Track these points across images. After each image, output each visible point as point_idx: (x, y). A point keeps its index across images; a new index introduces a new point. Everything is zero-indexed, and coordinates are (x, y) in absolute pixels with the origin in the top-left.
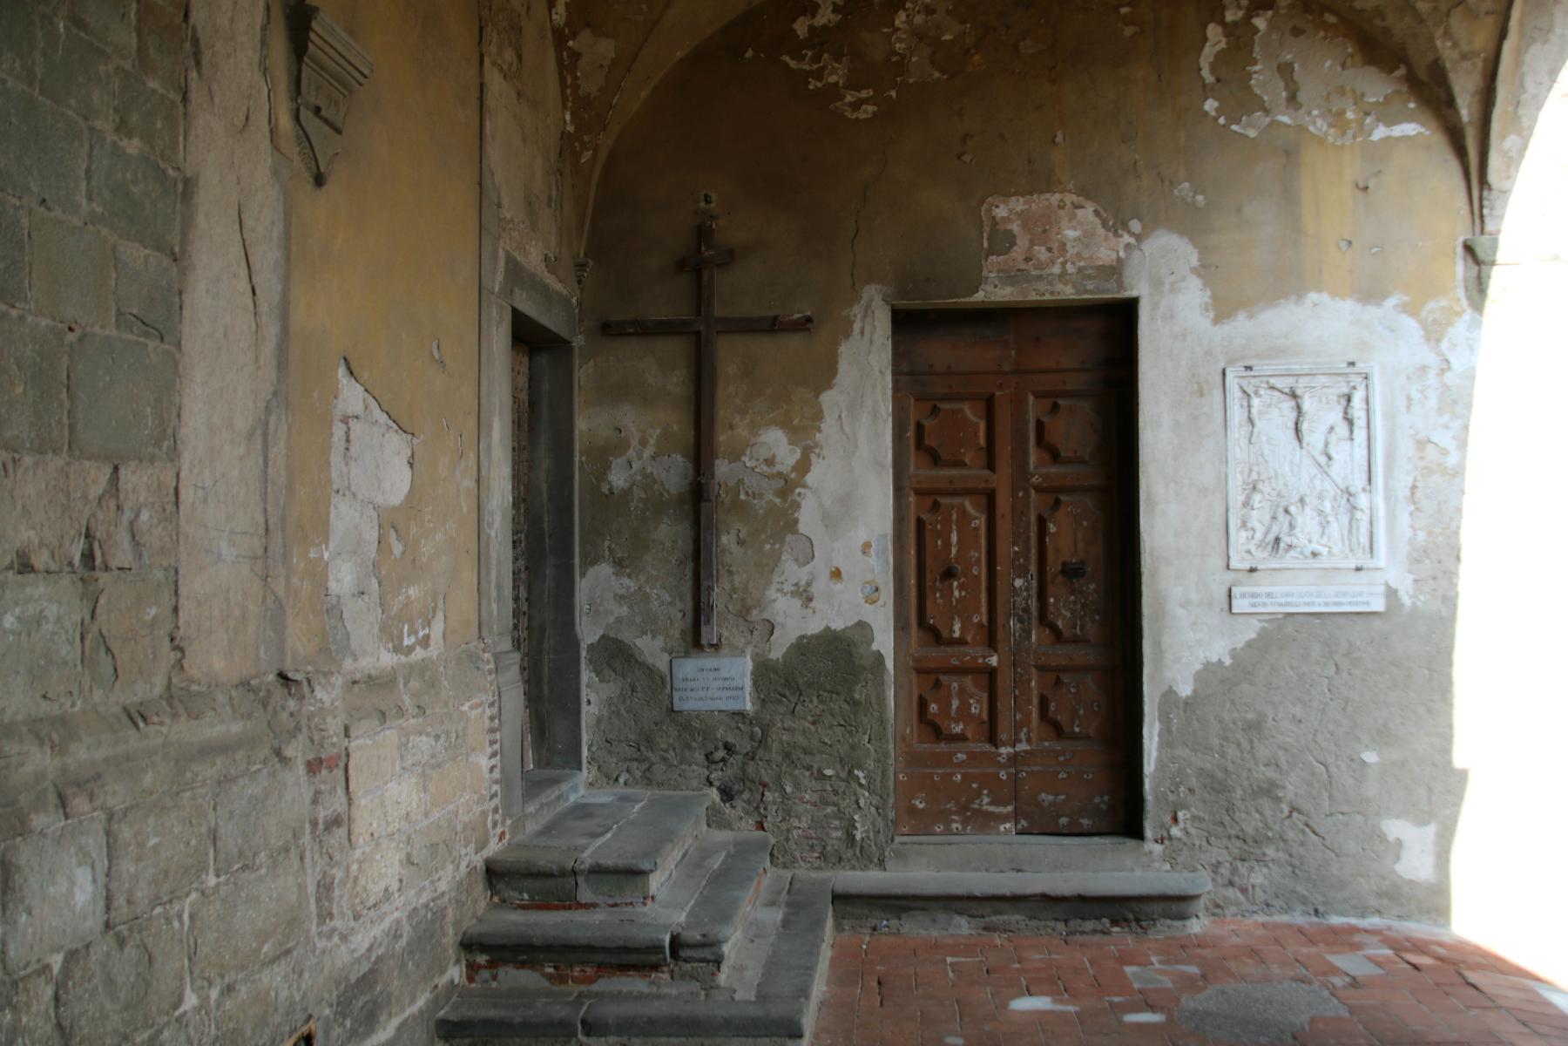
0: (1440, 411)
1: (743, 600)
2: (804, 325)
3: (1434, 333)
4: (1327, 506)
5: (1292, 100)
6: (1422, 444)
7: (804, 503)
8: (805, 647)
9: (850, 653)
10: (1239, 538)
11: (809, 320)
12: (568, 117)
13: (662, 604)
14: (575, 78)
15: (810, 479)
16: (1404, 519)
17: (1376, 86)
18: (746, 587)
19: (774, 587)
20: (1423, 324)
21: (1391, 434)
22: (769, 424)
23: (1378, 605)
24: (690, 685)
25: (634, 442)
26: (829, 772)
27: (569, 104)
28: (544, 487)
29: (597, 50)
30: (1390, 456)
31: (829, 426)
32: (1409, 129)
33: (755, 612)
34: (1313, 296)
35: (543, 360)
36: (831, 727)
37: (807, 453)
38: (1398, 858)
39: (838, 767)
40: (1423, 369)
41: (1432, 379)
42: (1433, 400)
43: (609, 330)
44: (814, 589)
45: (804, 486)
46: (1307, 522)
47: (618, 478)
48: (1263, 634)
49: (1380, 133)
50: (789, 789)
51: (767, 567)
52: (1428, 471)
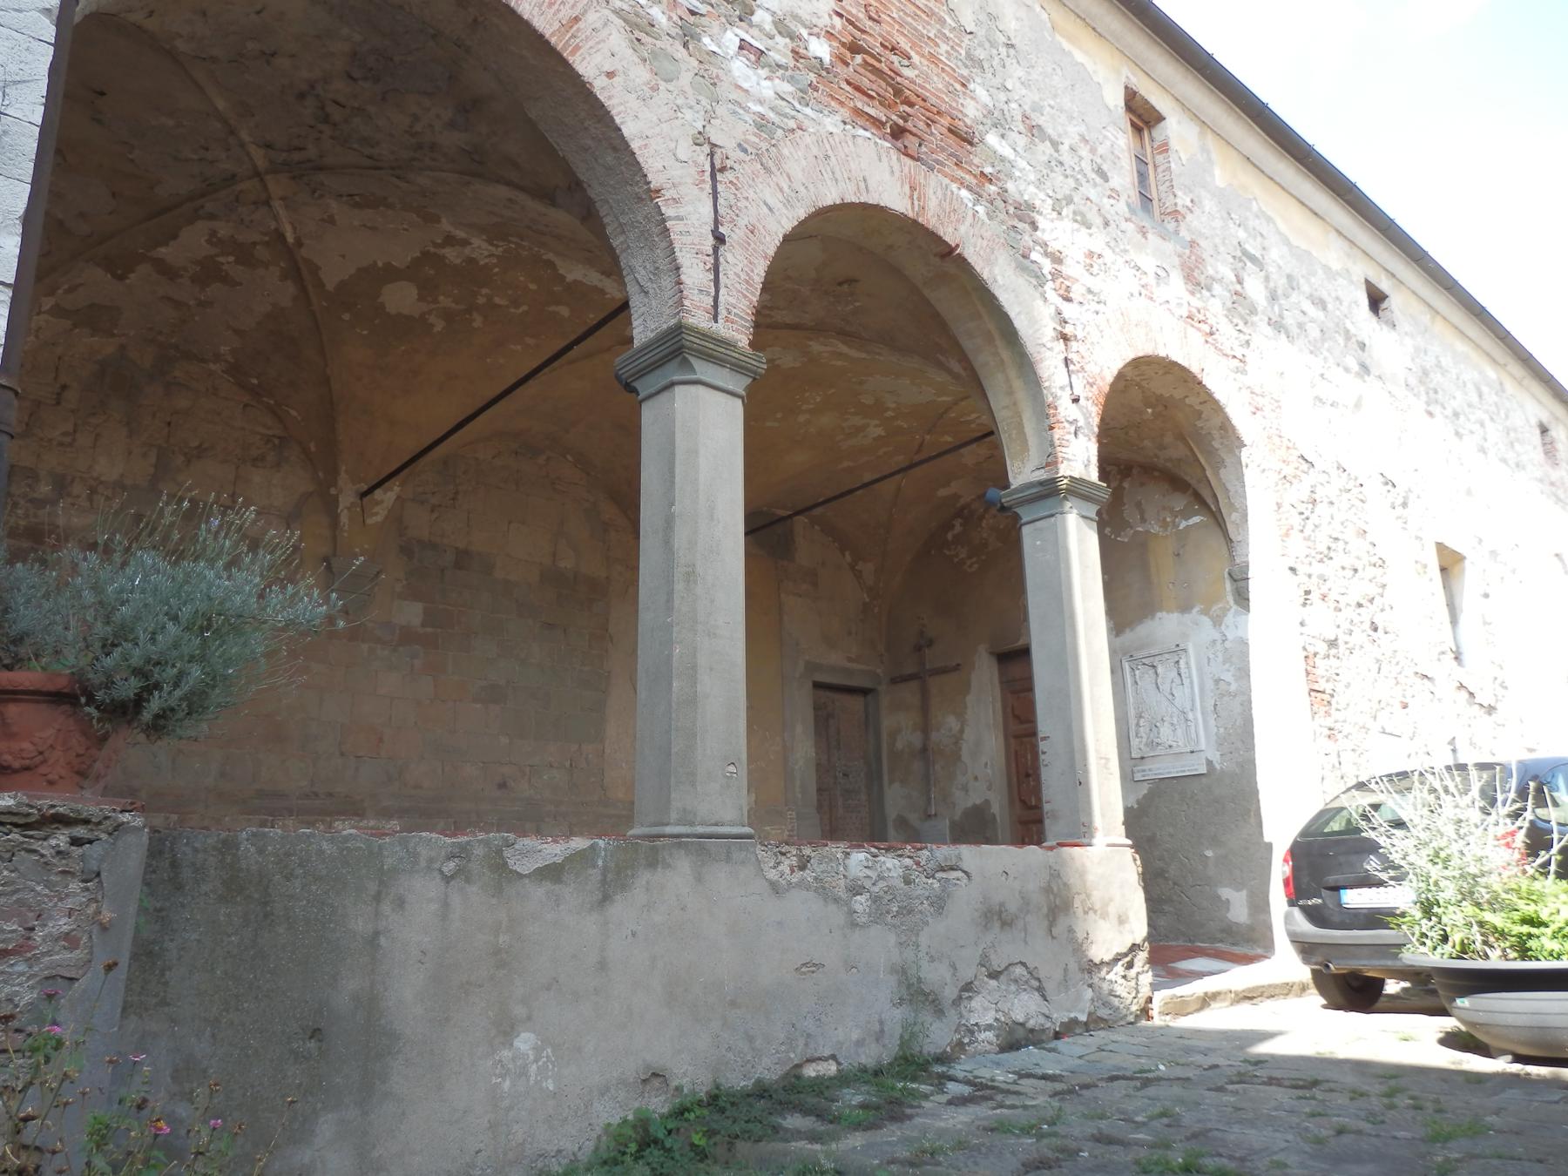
0: (1224, 663)
2: (957, 667)
3: (1217, 622)
4: (1175, 720)
5: (1143, 520)
6: (1217, 681)
10: (1135, 742)
16: (1212, 722)
17: (1179, 502)
20: (1212, 618)
23: (1203, 770)
29: (868, 568)
34: (1159, 615)
35: (869, 697)
38: (1228, 909)
41: (1219, 646)
42: (1220, 659)
43: (894, 681)
46: (1165, 731)
47: (899, 745)
49: (1183, 525)
52: (1222, 695)
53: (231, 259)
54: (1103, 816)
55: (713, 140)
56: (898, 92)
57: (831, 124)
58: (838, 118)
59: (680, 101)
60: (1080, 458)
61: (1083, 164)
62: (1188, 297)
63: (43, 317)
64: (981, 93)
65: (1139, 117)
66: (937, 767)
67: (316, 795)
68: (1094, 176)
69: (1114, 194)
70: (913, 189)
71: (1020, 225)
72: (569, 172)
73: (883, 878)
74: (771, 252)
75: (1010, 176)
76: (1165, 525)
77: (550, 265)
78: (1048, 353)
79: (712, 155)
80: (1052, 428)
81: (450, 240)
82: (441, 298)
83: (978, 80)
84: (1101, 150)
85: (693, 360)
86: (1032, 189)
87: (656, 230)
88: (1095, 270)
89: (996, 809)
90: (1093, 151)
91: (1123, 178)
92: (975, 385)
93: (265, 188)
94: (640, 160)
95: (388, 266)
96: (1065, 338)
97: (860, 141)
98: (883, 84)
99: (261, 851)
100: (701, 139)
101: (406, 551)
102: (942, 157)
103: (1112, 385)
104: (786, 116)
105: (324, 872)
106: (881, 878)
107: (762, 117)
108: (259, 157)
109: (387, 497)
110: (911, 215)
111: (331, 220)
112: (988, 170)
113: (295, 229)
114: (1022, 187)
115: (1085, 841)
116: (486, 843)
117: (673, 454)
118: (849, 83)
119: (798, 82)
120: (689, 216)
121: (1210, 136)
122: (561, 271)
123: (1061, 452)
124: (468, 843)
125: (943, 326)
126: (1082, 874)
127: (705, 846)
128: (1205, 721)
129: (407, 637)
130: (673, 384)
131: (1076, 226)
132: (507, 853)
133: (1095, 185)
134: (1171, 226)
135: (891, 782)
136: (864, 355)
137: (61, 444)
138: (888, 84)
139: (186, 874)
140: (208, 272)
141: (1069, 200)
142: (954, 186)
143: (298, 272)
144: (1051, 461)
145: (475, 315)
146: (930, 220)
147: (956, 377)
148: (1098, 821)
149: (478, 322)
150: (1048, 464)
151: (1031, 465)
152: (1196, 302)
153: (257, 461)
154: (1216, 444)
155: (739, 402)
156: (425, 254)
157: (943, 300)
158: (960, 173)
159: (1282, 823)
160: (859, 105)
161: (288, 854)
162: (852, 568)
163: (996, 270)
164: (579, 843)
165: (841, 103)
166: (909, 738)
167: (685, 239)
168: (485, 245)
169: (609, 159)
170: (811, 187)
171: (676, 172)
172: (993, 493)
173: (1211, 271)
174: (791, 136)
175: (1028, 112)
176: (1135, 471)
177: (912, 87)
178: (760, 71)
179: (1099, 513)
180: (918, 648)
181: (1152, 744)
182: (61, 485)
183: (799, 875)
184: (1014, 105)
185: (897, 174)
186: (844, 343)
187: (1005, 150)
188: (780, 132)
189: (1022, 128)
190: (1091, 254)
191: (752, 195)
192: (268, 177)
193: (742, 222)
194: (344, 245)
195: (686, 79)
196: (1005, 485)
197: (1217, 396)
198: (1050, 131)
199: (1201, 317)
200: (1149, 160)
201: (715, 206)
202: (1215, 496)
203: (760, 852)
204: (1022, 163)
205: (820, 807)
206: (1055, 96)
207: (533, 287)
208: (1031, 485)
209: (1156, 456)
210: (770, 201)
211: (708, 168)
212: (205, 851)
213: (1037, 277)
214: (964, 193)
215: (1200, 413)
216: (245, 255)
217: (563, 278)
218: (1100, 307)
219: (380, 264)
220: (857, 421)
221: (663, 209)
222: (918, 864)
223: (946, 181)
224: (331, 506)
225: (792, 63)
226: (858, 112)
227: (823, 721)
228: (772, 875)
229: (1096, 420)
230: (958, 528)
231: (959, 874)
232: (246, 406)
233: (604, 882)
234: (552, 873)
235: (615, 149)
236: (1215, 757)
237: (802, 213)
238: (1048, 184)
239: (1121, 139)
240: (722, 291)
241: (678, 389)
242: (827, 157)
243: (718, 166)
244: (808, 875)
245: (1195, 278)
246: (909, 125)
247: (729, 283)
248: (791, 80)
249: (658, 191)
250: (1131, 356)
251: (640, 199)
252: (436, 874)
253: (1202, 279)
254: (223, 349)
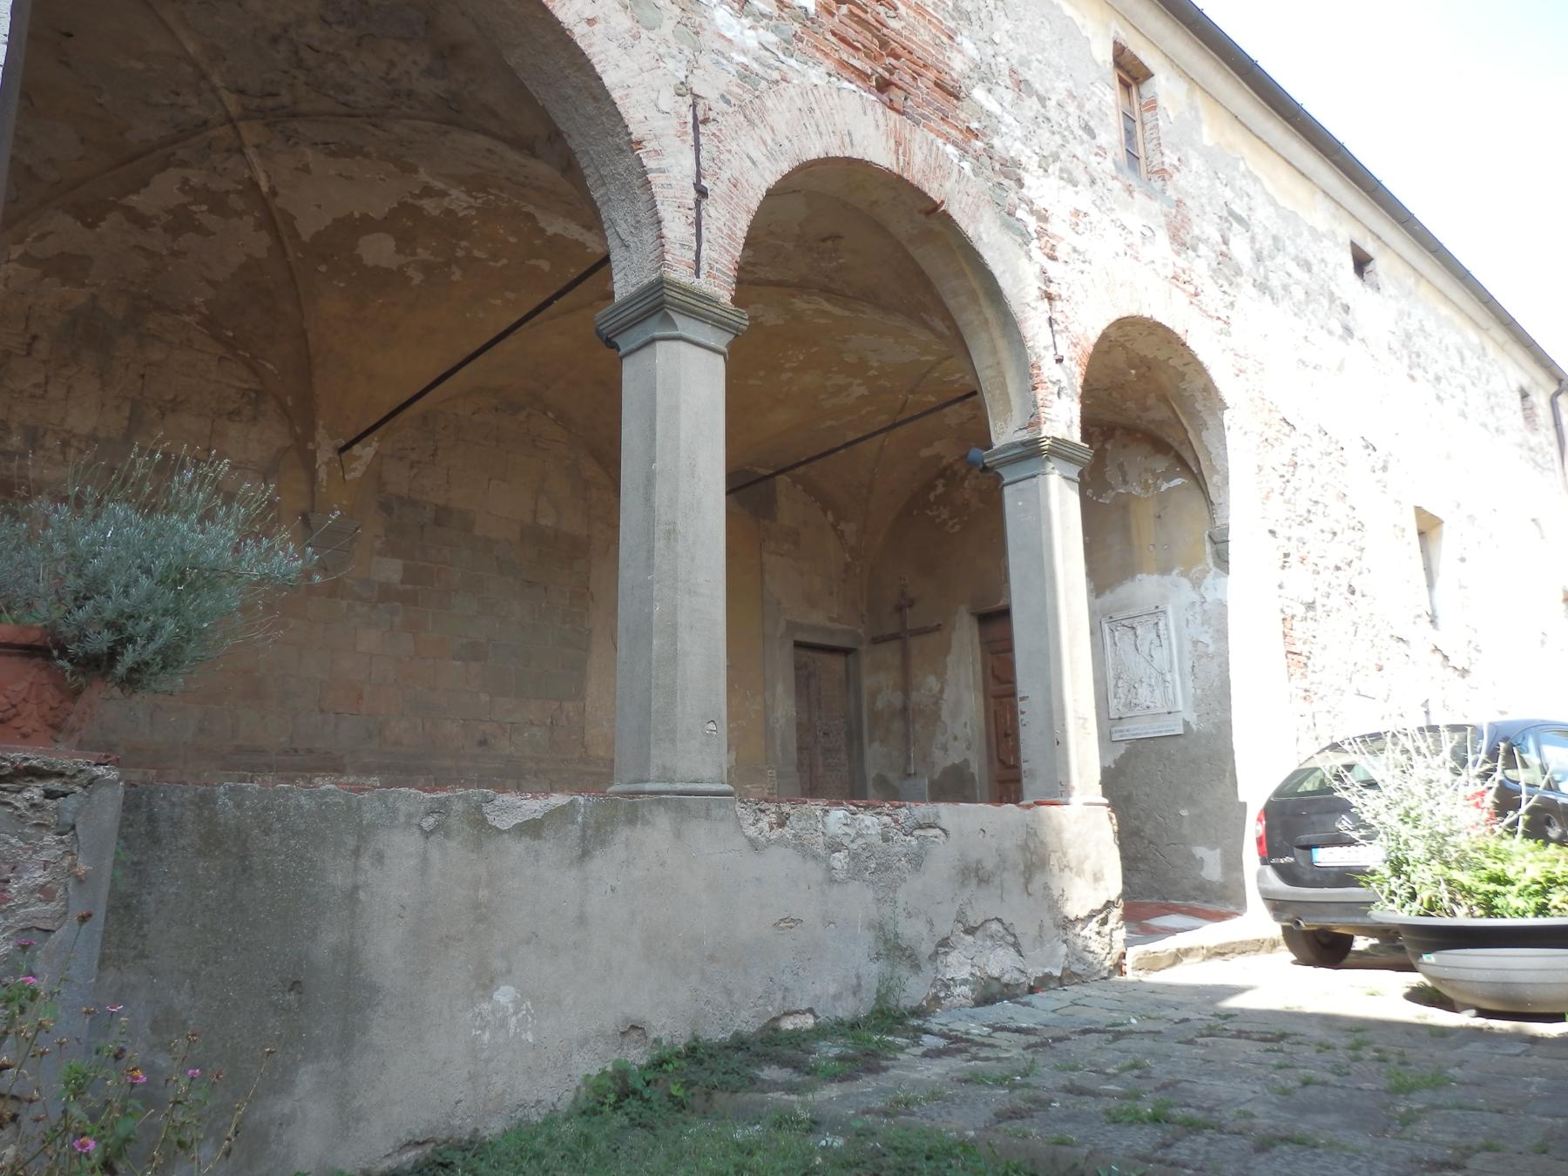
2: (938, 628)
3: (1197, 584)
5: (1125, 482)
6: (1196, 643)
10: (1113, 702)
16: (1190, 684)
17: (1161, 464)
20: (1191, 580)
21: (1179, 639)
29: (849, 528)
30: (1180, 652)
31: (949, 672)
32: (1178, 481)
35: (850, 657)
40: (1193, 603)
41: (1197, 608)
42: (1199, 620)
43: (876, 641)
46: (1143, 691)
47: (880, 705)
48: (1128, 752)
49: (1165, 487)
52: (1200, 657)
53: (204, 208)
54: (1080, 776)
55: (696, 91)
56: (884, 44)
57: (816, 75)
58: (823, 69)
59: (662, 50)
60: (1062, 418)
61: (1070, 120)
62: (1174, 257)
63: (11, 265)
64: (968, 46)
65: (1128, 73)
66: (917, 727)
67: (296, 751)
68: (1081, 132)
69: (1101, 152)
70: (898, 143)
71: (1006, 182)
72: (549, 122)
73: (862, 836)
74: (754, 206)
75: (996, 132)
76: (1146, 487)
77: (530, 217)
78: (1032, 313)
79: (694, 106)
80: (1035, 389)
81: (428, 191)
82: (419, 250)
83: (966, 33)
84: (1088, 106)
85: (674, 316)
86: (1018, 145)
87: (638, 182)
88: (1080, 229)
89: (975, 768)
90: (1080, 107)
91: (1111, 135)
92: (958, 343)
93: (238, 135)
94: (622, 110)
95: (365, 218)
96: (1050, 297)
97: (844, 93)
98: (869, 36)
99: (238, 806)
100: (683, 89)
101: (386, 507)
102: (927, 111)
103: (1096, 346)
104: (769, 67)
105: (303, 827)
106: (859, 835)
107: (746, 67)
108: (232, 103)
109: (365, 452)
110: (896, 170)
111: (306, 169)
112: (974, 125)
113: (269, 177)
114: (1009, 143)
115: (1061, 800)
116: (466, 799)
117: (654, 411)
118: (834, 34)
119: (782, 32)
120: (671, 168)
121: (1198, 93)
122: (542, 224)
123: (1045, 413)
124: (447, 799)
125: (927, 284)
126: (1059, 832)
127: (684, 803)
128: (1183, 684)
129: (386, 593)
130: (654, 340)
131: (1062, 183)
132: (487, 808)
133: (1082, 142)
134: (1158, 185)
135: (871, 741)
136: (847, 313)
137: (32, 396)
138: (874, 36)
139: (164, 828)
140: (181, 222)
141: (1056, 157)
142: (940, 142)
143: (274, 222)
144: (1034, 422)
145: (454, 268)
146: (915, 175)
147: (940, 336)
148: (1075, 780)
149: (457, 275)
150: (1031, 425)
151: (1013, 426)
152: (1181, 262)
153: (233, 415)
154: (1199, 407)
155: (721, 360)
156: (403, 206)
157: (926, 256)
158: (946, 128)
159: (1256, 785)
160: (845, 57)
161: (265, 809)
162: (834, 527)
163: (982, 228)
164: (558, 799)
165: (826, 54)
166: (889, 698)
167: (668, 192)
168: (463, 196)
169: (590, 109)
170: (795, 140)
171: (658, 123)
172: (975, 453)
173: (1197, 232)
174: (775, 88)
175: (1016, 67)
176: (1117, 433)
177: (898, 38)
178: (744, 20)
179: (1081, 474)
180: (899, 609)
181: (1130, 705)
182: (33, 438)
183: (778, 832)
184: (1001, 59)
185: (882, 128)
186: (827, 300)
187: (991, 104)
188: (763, 84)
189: (1009, 82)
190: (1076, 213)
191: (734, 148)
192: (241, 124)
193: (725, 175)
194: (320, 194)
195: (668, 27)
196: (988, 445)
197: (1200, 358)
198: (1037, 86)
199: (1187, 278)
200: (1137, 118)
201: (697, 159)
202: (1197, 459)
203: (739, 808)
204: (1008, 119)
205: (800, 765)
206: (1044, 50)
207: (513, 240)
208: (1014, 445)
209: (1139, 417)
210: (754, 155)
211: (690, 119)
212: (182, 805)
213: (1022, 235)
214: (950, 149)
215: (1182, 376)
216: (218, 204)
217: (543, 231)
218: (1085, 267)
219: (357, 215)
220: (840, 380)
221: (645, 161)
222: (896, 821)
223: (932, 136)
224: (308, 461)
225: (776, 13)
226: (843, 64)
227: (804, 682)
228: (752, 832)
229: (1079, 381)
230: (940, 490)
231: (937, 832)
232: (221, 359)
233: (583, 838)
234: (531, 828)
235: (596, 99)
236: (1192, 718)
237: (786, 168)
238: (1035, 140)
239: (1108, 95)
240: (704, 246)
241: (660, 345)
242: (811, 110)
243: (700, 118)
244: (787, 832)
245: (1181, 239)
246: (895, 79)
247: (711, 237)
248: (776, 30)
249: (639, 143)
250: (1117, 317)
251: (622, 151)
252: (415, 829)
253: (1188, 239)
254: (197, 300)
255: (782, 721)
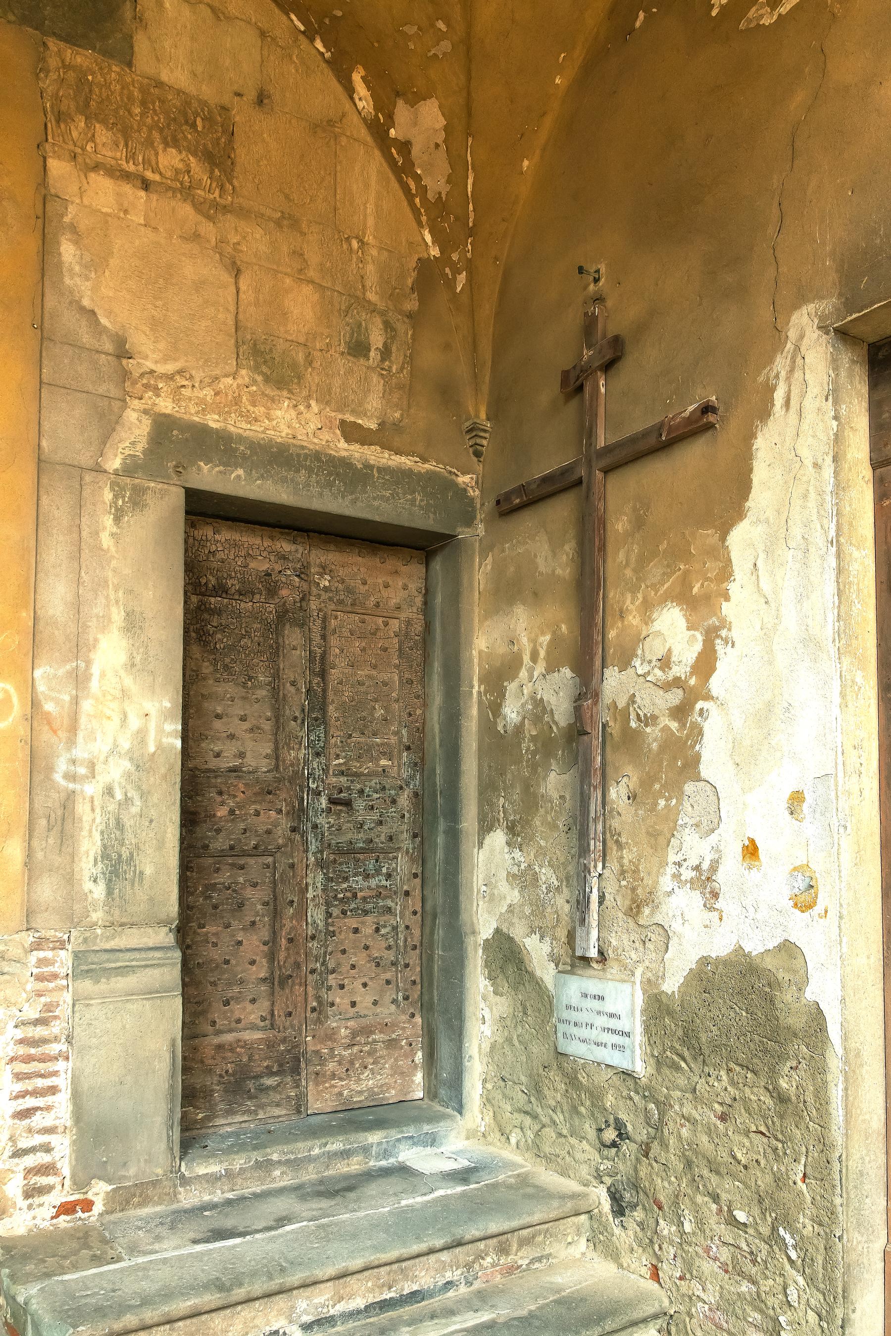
1: (634, 889)
2: (702, 422)
7: (707, 727)
8: (707, 976)
9: (771, 1001)
11: (707, 409)
12: (428, 238)
13: (549, 891)
14: (418, 178)
15: (715, 684)
18: (636, 871)
19: (671, 870)
22: (663, 601)
24: (574, 1016)
25: (526, 658)
26: (741, 1216)
27: (424, 219)
28: (437, 730)
33: (647, 911)
36: (747, 1133)
37: (711, 636)
39: (756, 1211)
44: (721, 876)
45: (708, 697)
50: (688, 1227)
51: (660, 836)
166: (540, 689)
255: (115, 772)
